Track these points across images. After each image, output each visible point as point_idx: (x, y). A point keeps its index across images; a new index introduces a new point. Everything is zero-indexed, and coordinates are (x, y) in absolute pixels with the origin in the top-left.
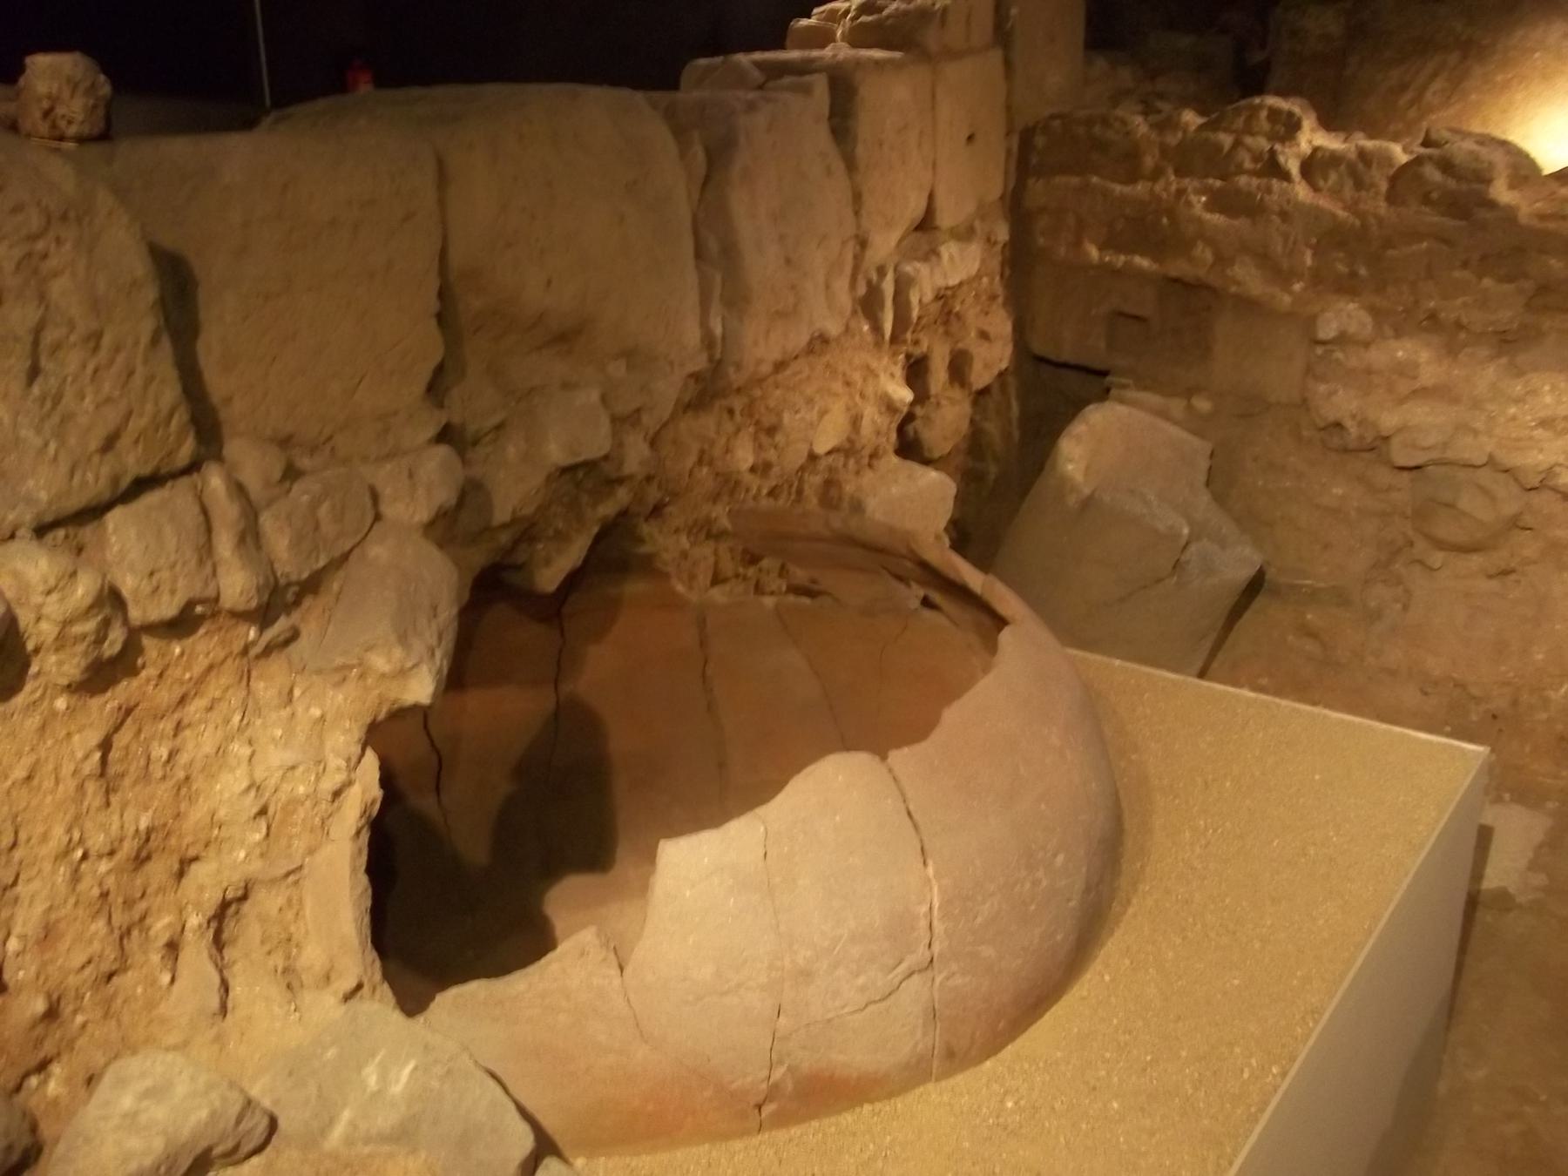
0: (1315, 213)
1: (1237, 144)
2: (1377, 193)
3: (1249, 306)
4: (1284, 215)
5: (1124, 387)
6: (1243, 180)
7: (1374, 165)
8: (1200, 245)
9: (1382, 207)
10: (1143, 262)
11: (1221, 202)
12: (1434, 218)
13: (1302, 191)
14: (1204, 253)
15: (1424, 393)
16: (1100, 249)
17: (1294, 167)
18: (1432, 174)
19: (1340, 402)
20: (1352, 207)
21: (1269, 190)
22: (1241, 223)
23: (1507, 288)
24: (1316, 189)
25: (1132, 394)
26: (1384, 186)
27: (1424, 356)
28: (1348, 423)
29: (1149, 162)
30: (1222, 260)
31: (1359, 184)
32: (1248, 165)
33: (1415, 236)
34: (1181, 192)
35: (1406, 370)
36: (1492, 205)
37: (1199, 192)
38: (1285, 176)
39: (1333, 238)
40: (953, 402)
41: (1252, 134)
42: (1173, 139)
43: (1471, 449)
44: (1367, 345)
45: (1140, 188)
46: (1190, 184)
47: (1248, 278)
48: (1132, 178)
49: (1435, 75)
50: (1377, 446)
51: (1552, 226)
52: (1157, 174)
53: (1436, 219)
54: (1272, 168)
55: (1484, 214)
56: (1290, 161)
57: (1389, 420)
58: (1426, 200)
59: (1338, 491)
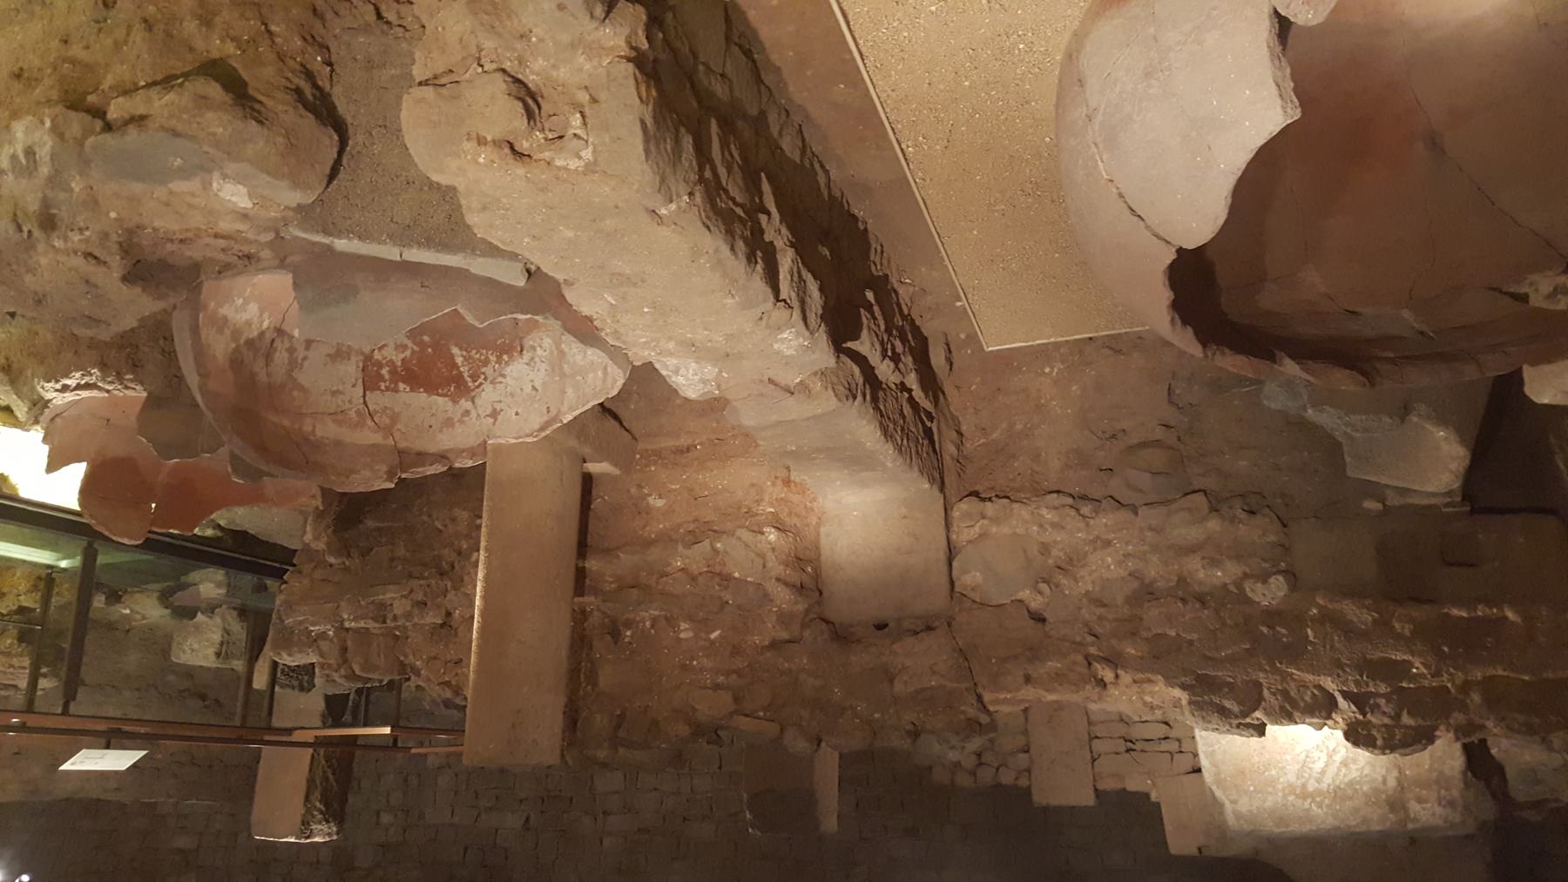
1: (1397, 717)
2: (1269, 689)
4: (1340, 666)
5: (1447, 505)
6: (1383, 688)
7: (1277, 708)
8: (1407, 632)
12: (1223, 674)
13: (1330, 684)
15: (1192, 549)
16: (1506, 618)
20: (1285, 677)
21: (1357, 683)
22: (1376, 655)
24: (1319, 687)
26: (1266, 693)
27: (1201, 575)
28: (1243, 515)
29: (1476, 697)
30: (1383, 625)
31: (1285, 694)
32: (1382, 702)
33: (1232, 660)
34: (1437, 674)
35: (1214, 562)
36: (1184, 687)
37: (1422, 676)
38: (1346, 695)
39: (1295, 652)
41: (1386, 726)
43: (1149, 516)
44: (1246, 576)
45: (1478, 675)
47: (1358, 614)
48: (1489, 680)
49: (1323, 772)
50: (1216, 505)
51: (1140, 676)
52: (1465, 687)
53: (1220, 674)
54: (1358, 700)
55: (1188, 680)
56: (1347, 706)
57: (1213, 524)
58: (1231, 686)
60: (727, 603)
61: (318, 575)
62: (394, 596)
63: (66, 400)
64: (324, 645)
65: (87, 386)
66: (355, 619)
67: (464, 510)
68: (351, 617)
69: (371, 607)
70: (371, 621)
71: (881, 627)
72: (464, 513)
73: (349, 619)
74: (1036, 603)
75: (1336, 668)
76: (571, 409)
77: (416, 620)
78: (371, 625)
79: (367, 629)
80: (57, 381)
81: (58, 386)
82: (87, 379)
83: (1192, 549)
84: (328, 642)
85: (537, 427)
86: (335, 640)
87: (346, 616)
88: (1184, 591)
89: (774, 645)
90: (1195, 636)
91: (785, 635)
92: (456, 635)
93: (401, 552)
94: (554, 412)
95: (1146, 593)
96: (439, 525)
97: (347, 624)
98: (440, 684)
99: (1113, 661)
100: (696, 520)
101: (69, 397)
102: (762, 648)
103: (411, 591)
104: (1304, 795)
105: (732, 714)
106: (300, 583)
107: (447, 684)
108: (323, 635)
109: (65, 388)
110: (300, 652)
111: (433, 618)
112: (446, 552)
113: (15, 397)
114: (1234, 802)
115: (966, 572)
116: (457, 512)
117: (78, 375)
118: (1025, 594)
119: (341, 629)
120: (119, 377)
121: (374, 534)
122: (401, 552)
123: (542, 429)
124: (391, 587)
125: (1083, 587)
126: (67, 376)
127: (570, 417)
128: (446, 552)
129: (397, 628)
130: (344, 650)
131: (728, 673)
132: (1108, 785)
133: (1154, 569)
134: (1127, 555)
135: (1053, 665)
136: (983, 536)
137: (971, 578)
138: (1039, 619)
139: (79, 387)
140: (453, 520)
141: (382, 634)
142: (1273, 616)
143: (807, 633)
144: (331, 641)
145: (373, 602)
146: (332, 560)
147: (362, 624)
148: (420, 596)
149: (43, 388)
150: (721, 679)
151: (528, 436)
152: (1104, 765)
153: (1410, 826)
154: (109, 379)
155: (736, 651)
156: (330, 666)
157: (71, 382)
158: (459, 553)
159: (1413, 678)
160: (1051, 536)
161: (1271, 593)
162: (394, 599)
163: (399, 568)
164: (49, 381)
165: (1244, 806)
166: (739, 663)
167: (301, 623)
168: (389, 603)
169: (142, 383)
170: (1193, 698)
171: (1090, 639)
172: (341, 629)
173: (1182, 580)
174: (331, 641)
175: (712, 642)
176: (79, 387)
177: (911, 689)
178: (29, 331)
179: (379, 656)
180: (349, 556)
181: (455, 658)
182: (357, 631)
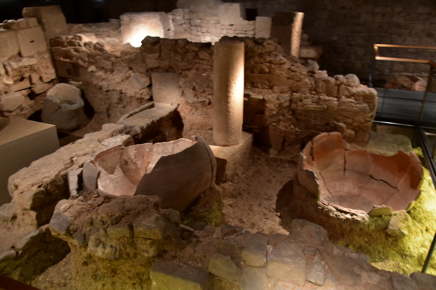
0: (86, 52)
3: (83, 67)
5: (70, 81)
9: (93, 50)
10: (68, 60)
11: (76, 50)
12: (99, 52)
14: (74, 58)
15: (103, 79)
17: (82, 44)
18: (97, 46)
19: (95, 82)
20: (90, 50)
23: (109, 63)
25: (72, 82)
30: (77, 60)
36: (104, 50)
39: (89, 56)
40: (41, 84)
42: (68, 40)
43: (111, 88)
46: (71, 47)
47: (80, 62)
55: (104, 52)
57: (100, 84)
59: (101, 96)
60: (197, 83)
61: (350, 121)
62: (311, 106)
63: (357, 210)
64: (347, 93)
65: (341, 211)
66: (329, 100)
67: (281, 129)
68: (331, 101)
69: (321, 103)
70: (322, 98)
71: (167, 71)
72: (281, 128)
73: (333, 101)
74: (130, 72)
75: (83, 52)
76: (169, 144)
77: (304, 96)
78: (324, 97)
79: (328, 96)
80: (353, 219)
81: (354, 217)
82: (339, 213)
83: (103, 79)
84: (345, 94)
85: (180, 142)
86: (341, 94)
87: (336, 102)
88: (106, 71)
89: (189, 70)
90: (104, 61)
91: (186, 72)
92: (290, 88)
93: (313, 121)
94: (176, 144)
95: (112, 71)
96: (292, 126)
97: (335, 99)
98: (296, 72)
99: (116, 57)
100: (207, 108)
101: (353, 211)
102: (192, 69)
103: (303, 106)
104: (144, 22)
105: (199, 51)
106: (359, 119)
107: (293, 71)
108: (348, 97)
109: (352, 215)
110: (358, 92)
111: (296, 95)
112: (289, 117)
113: (391, 223)
114: (157, 21)
115: (145, 82)
116: (284, 129)
117: (342, 217)
118: (133, 74)
119: (339, 98)
120: (323, 209)
121: (323, 130)
122: (313, 121)
123: (178, 141)
124: (312, 109)
125: (121, 74)
126: (347, 219)
127: (171, 142)
128: (289, 117)
129: (314, 94)
130: (338, 90)
131: (199, 63)
132: (251, 22)
133: (110, 76)
134: (114, 80)
135: (127, 57)
136: (140, 90)
137: (145, 81)
138: (131, 68)
139: (346, 213)
140: (285, 127)
141: (321, 93)
142: (91, 63)
143: (180, 71)
144: (343, 94)
145: (321, 105)
146: (341, 124)
147: (327, 98)
148: (300, 103)
149: (364, 219)
150: (201, 62)
151: (182, 140)
152: (252, 28)
153: (129, 15)
154: (327, 210)
155: (198, 69)
156: (345, 85)
157: (348, 216)
158: (284, 115)
159: (73, 49)
160: (127, 87)
161: (92, 68)
162: (311, 105)
163: (313, 115)
164: (357, 220)
165: (155, 20)
166: (197, 66)
167: (359, 104)
168: (314, 104)
169: (317, 204)
170: (102, 47)
171: (120, 62)
172: (339, 98)
173: (106, 72)
174: (343, 94)
175: (204, 72)
176: (346, 213)
177: (155, 54)
178: (370, 245)
179: (322, 86)
180: (334, 124)
181: (290, 80)
182: (332, 96)
